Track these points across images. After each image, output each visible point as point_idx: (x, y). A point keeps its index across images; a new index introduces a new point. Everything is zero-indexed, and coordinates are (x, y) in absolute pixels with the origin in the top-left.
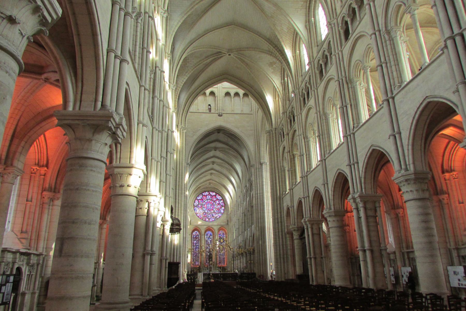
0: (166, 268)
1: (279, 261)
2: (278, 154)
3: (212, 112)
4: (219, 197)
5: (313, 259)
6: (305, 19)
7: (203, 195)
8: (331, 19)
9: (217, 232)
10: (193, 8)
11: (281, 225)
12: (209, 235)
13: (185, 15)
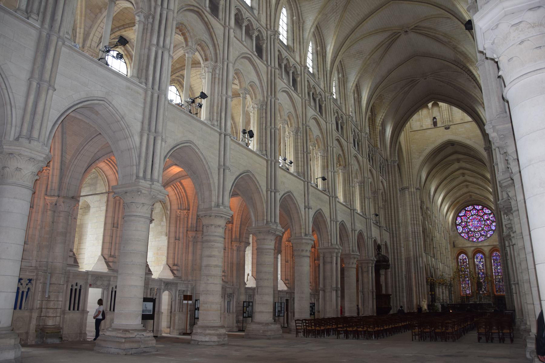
0: (373, 299)
3: (438, 125)
4: (487, 211)
7: (466, 210)
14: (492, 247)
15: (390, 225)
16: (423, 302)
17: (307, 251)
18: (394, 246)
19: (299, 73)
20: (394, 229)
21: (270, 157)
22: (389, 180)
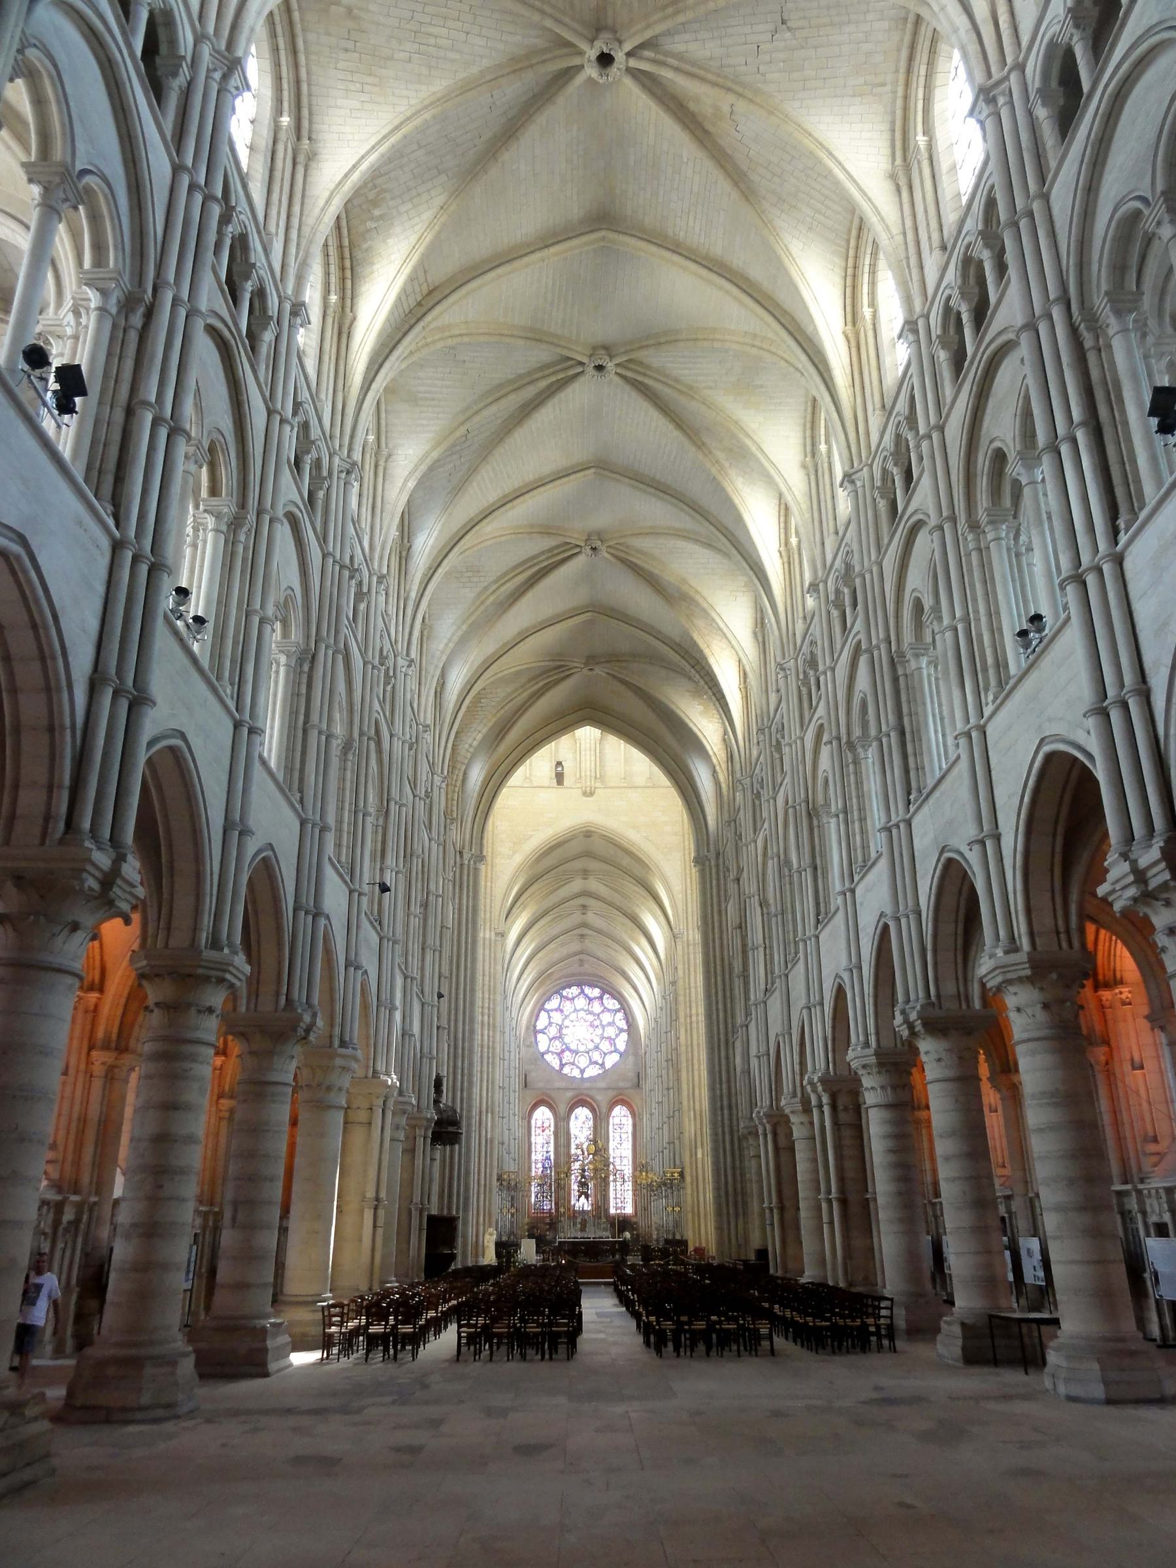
0: (420, 1230)
1: (725, 1211)
3: (566, 782)
7: (562, 996)
9: (604, 1110)
10: (483, 603)
11: (731, 1115)
12: (582, 1118)
13: (464, 622)
14: (615, 1092)
15: (452, 1023)
16: (487, 1237)
17: (340, 1089)
19: (365, 590)
20: (460, 1035)
22: (460, 904)
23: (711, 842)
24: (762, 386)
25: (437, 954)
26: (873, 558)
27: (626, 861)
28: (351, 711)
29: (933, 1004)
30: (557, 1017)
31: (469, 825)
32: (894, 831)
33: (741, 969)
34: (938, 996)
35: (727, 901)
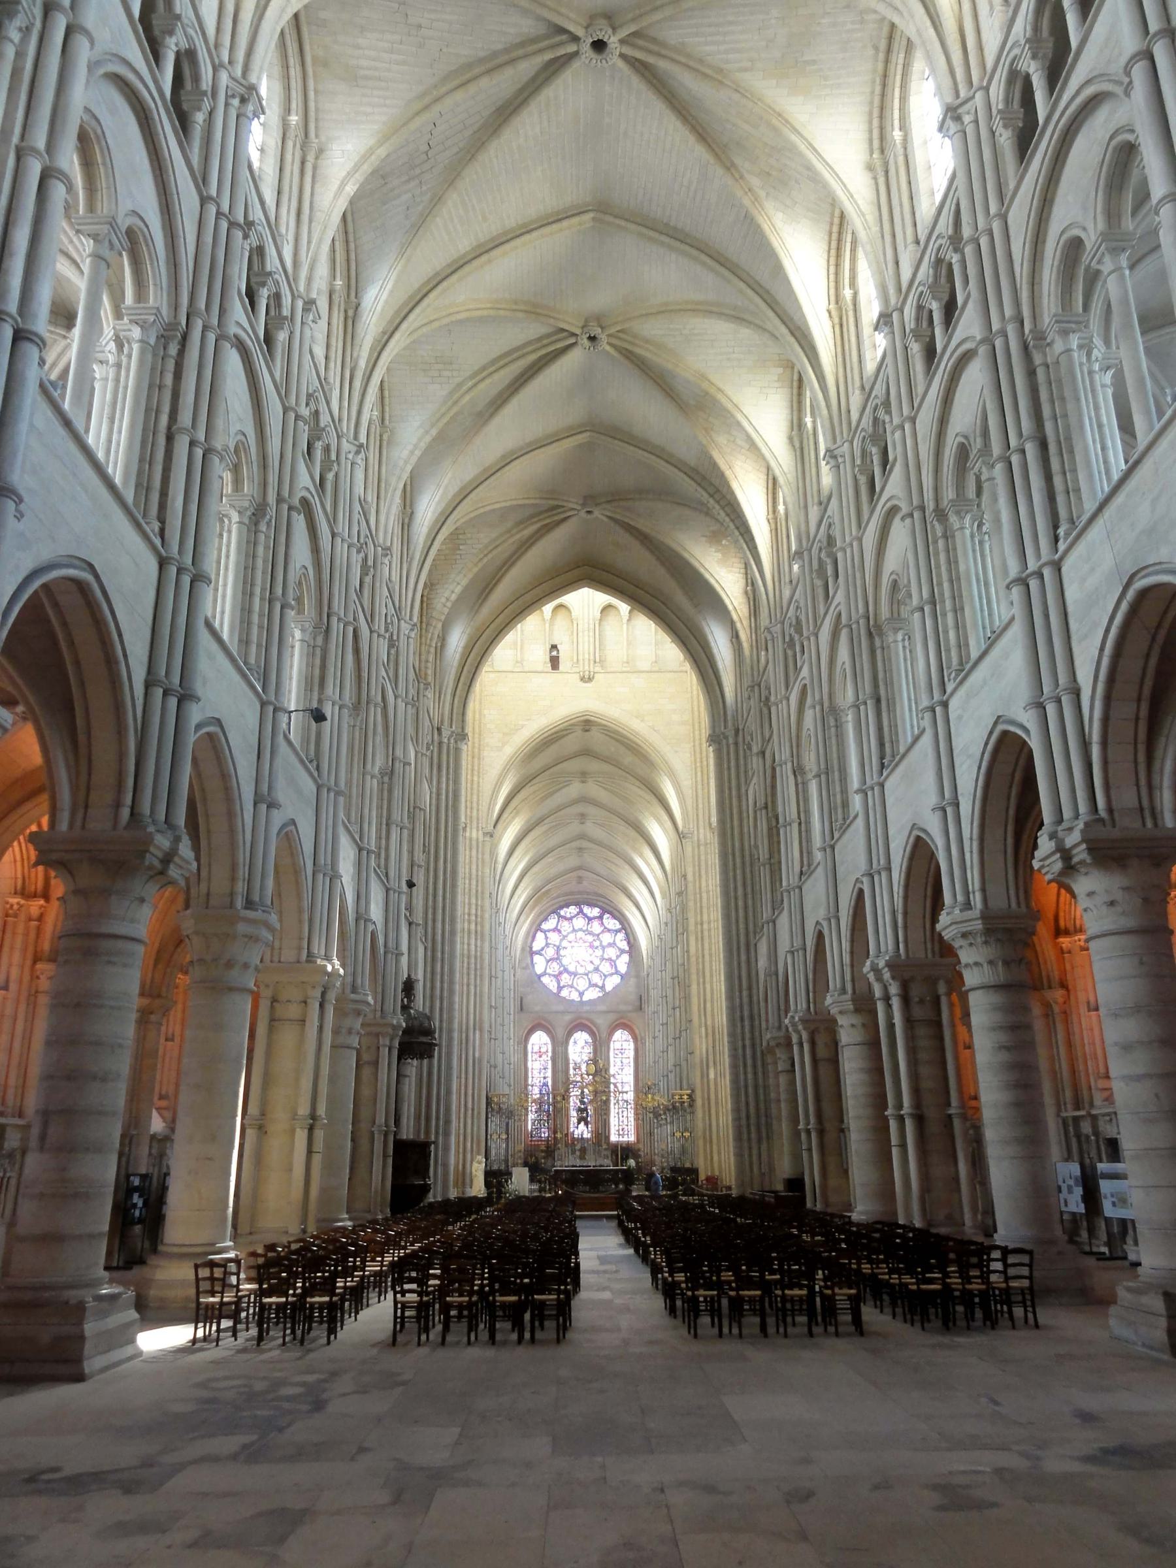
0: (385, 1156)
1: (745, 1136)
2: (744, 807)
5: (814, 1135)
6: (789, 417)
7: (560, 916)
8: (835, 442)
9: (604, 1035)
10: (456, 403)
11: (752, 1027)
12: (581, 1043)
13: (433, 426)
15: (430, 923)
16: (475, 1165)
17: (246, 966)
18: (433, 988)
19: (286, 312)
21: (175, 548)
23: (729, 718)
24: (814, 62)
25: (405, 832)
26: (993, 209)
27: (628, 759)
28: (264, 466)
29: (1102, 820)
30: (554, 938)
31: (449, 697)
32: (1034, 584)
33: (767, 856)
34: (1110, 810)
35: (747, 784)
